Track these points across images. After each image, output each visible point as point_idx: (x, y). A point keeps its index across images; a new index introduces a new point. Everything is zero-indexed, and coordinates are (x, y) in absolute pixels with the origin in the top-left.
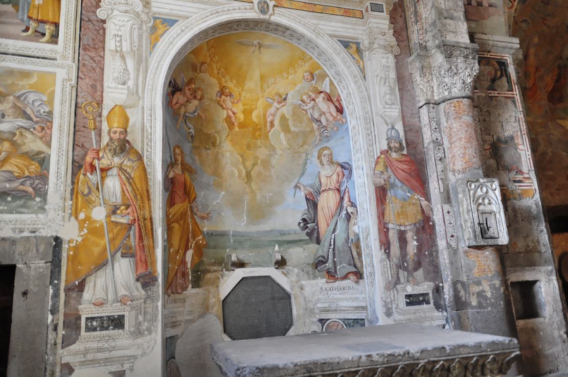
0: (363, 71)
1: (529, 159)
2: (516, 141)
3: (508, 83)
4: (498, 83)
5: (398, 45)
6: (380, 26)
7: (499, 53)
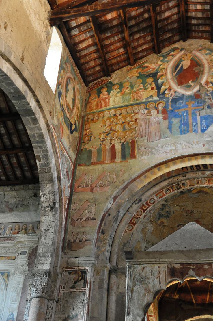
0: (6, 286)
2: (79, 317)
3: (84, 283)
4: (78, 283)
5: (28, 270)
6: (21, 262)
7: (84, 266)
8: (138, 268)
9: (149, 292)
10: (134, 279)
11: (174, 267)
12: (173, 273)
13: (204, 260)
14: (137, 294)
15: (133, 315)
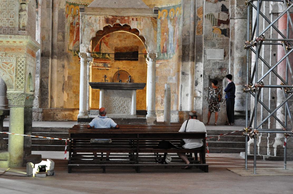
1: (39, 36)
3: (37, 5)
8: (87, 17)
9: (93, 32)
10: (84, 24)
11: (108, 18)
12: (107, 20)
13: (126, 14)
14: (86, 32)
15: (84, 43)
